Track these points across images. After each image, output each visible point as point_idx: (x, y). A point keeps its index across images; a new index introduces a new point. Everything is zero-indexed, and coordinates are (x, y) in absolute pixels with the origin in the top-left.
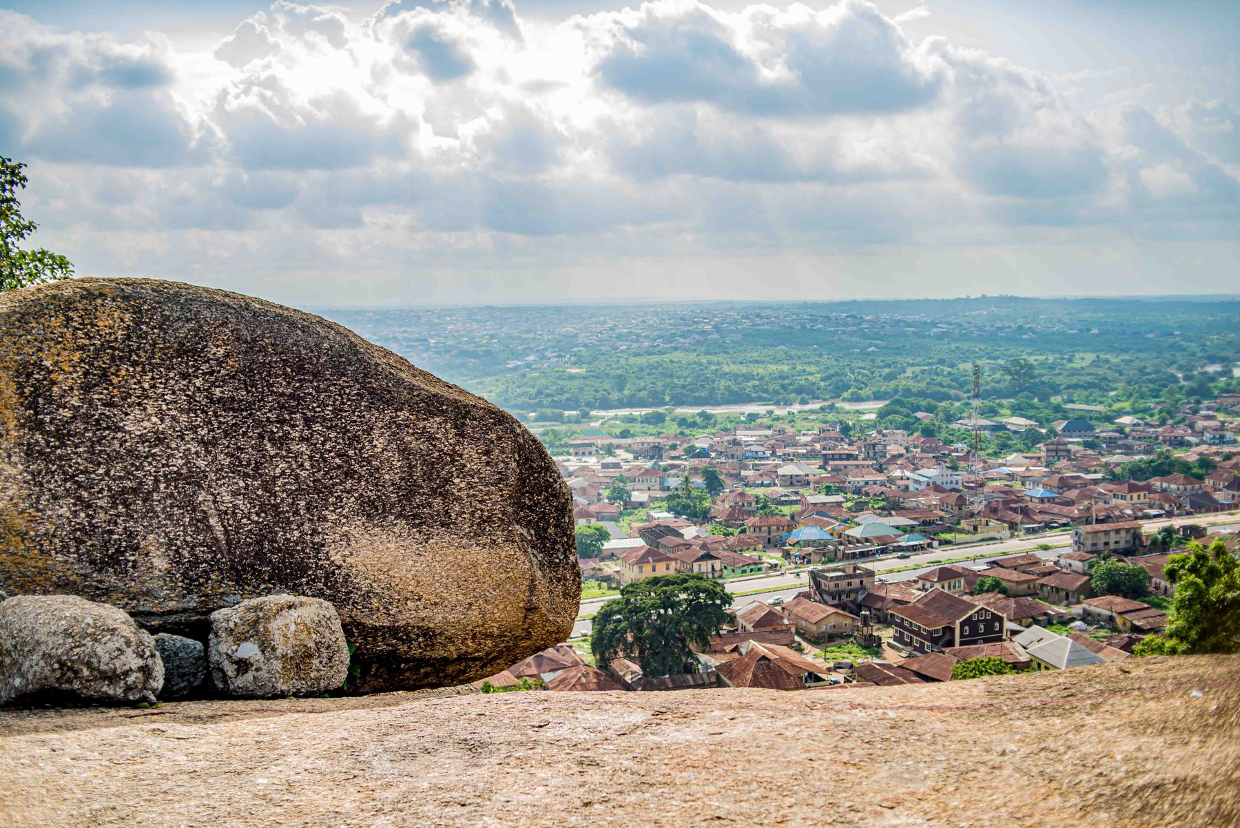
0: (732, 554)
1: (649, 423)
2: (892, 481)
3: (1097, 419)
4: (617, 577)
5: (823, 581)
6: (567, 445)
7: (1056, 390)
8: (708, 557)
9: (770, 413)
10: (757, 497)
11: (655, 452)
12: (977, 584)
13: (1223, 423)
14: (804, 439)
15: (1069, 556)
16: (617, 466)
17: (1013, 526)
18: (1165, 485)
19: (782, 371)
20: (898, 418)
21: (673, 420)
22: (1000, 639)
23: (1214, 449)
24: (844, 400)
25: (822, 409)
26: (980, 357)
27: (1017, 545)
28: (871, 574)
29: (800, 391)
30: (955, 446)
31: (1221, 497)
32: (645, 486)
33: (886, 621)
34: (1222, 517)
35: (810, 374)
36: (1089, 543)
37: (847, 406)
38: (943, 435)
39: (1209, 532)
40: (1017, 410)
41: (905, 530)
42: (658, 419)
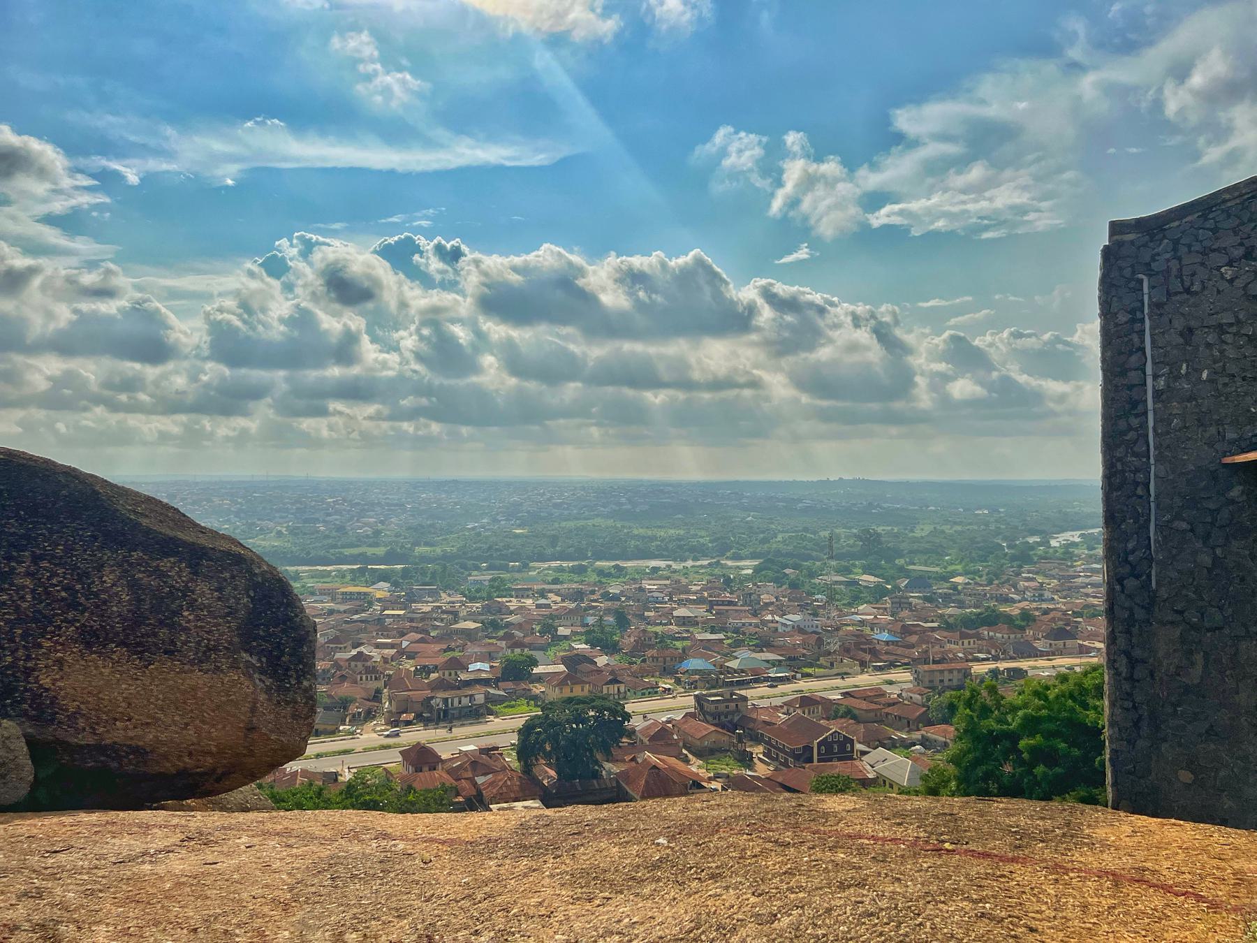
0: (634, 679)
1: (573, 572)
2: (764, 623)
3: (935, 578)
4: (542, 696)
5: (705, 703)
6: (510, 589)
7: (900, 555)
8: (615, 681)
9: (670, 566)
10: (656, 633)
11: (578, 596)
12: (831, 710)
13: (1042, 584)
14: (694, 588)
15: (909, 690)
16: (548, 606)
17: (863, 664)
18: (991, 634)
20: (770, 573)
21: (593, 571)
22: (851, 758)
23: (1034, 605)
24: (727, 558)
26: (836, 527)
27: (865, 680)
28: (745, 699)
30: (817, 597)
31: (1040, 645)
32: (569, 623)
33: (757, 739)
34: (1041, 663)
36: (926, 680)
37: (730, 563)
38: (807, 587)
39: (1030, 673)
40: (867, 570)
41: (774, 664)
42: (581, 570)
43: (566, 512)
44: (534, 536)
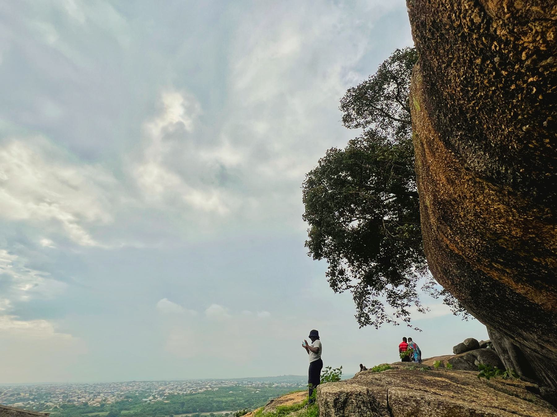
19: (232, 400)
29: (239, 406)
43: (185, 393)
44: (173, 403)
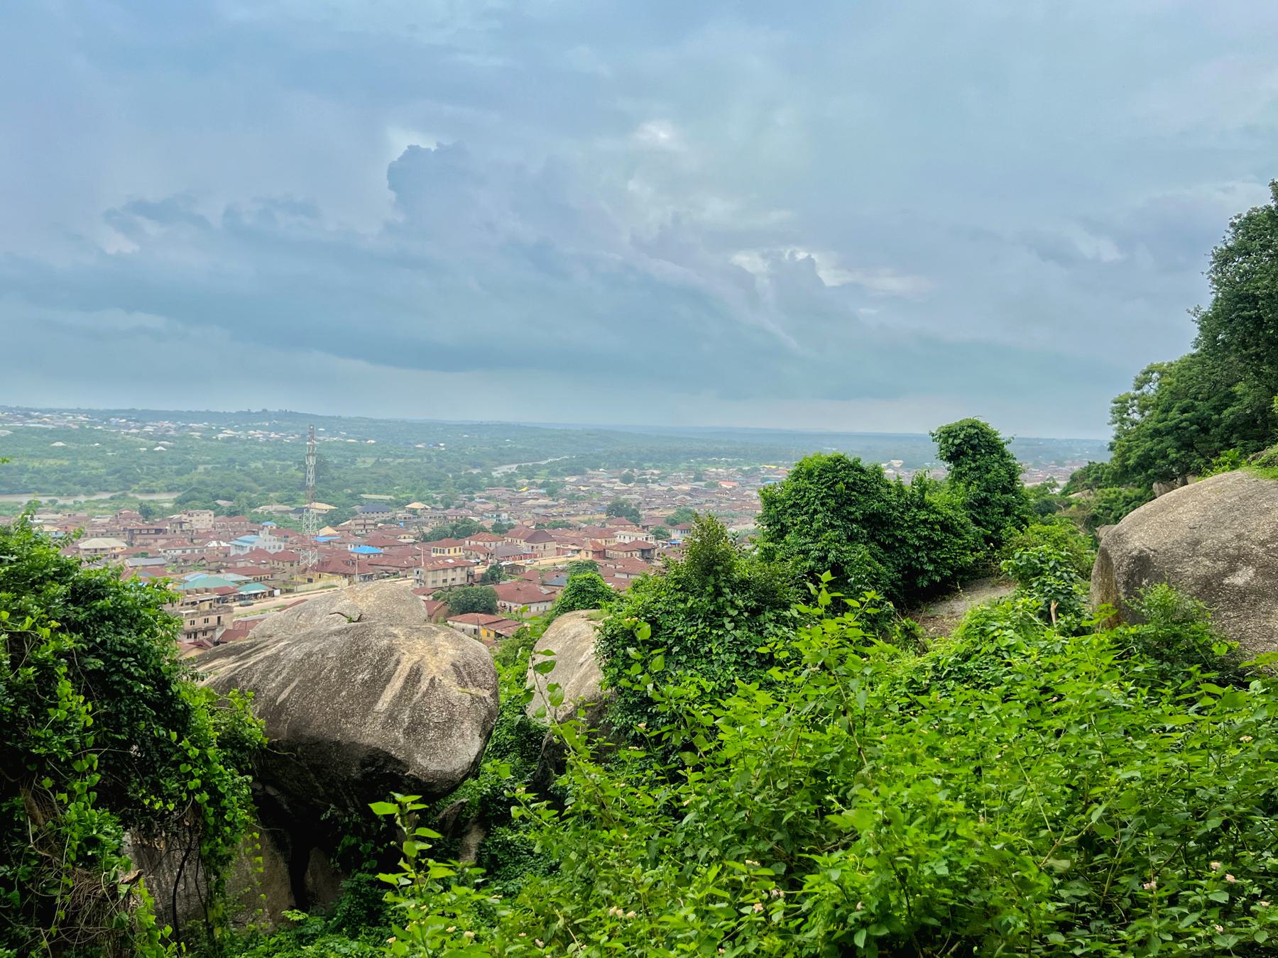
25: (112, 498)
29: (84, 483)
35: (93, 468)
